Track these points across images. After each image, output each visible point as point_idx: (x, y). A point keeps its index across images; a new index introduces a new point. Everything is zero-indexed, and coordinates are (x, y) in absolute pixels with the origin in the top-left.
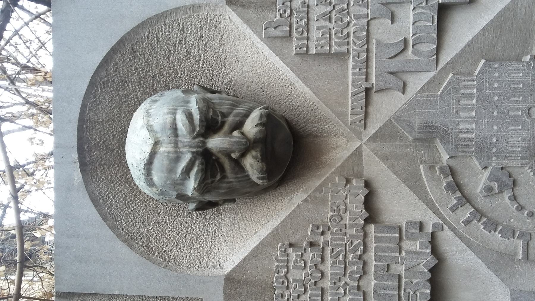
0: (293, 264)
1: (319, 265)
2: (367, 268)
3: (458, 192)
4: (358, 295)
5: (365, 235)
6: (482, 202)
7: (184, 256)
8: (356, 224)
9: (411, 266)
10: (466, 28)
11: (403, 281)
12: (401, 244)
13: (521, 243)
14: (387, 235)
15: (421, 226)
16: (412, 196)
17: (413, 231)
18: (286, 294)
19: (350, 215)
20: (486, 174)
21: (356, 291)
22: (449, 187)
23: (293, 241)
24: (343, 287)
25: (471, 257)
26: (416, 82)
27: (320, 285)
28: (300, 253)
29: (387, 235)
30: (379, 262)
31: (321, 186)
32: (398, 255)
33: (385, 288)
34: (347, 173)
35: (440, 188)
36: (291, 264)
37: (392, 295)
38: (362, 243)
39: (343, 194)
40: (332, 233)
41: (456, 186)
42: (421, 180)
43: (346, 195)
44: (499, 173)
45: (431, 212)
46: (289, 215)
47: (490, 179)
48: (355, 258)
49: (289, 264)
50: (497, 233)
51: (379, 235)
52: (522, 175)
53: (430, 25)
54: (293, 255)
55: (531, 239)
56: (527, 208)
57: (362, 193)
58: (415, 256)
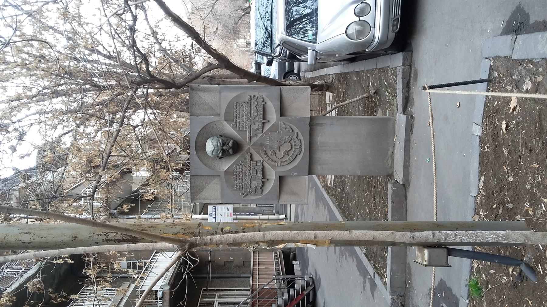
6: (271, 157)
10: (268, 127)
26: (259, 136)
53: (261, 126)
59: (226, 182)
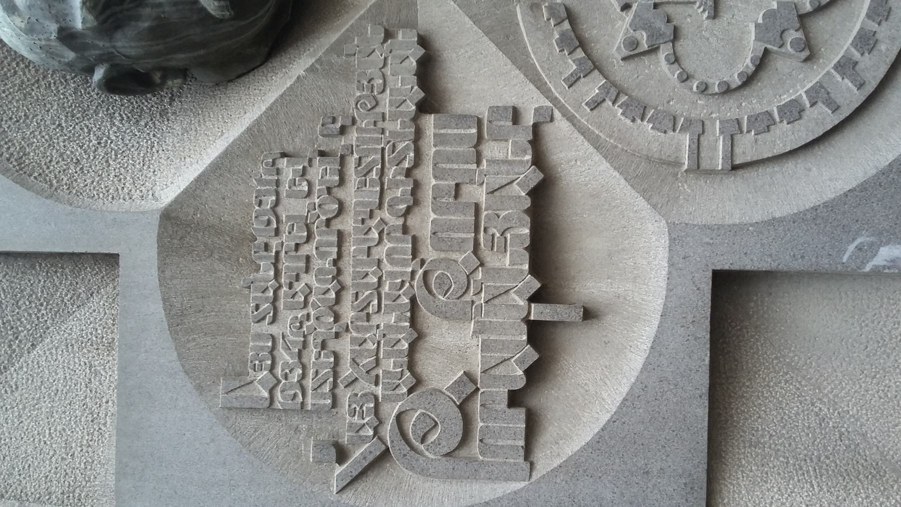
0: (287, 188)
1: (335, 190)
2: (420, 195)
3: (579, 50)
4: (403, 241)
5: (418, 134)
6: (623, 72)
7: (89, 181)
8: (401, 112)
9: (497, 186)
11: (484, 214)
12: (480, 148)
13: (686, 140)
14: (455, 131)
15: (516, 115)
16: (500, 60)
17: (502, 123)
18: (274, 243)
19: (391, 95)
20: (629, 17)
21: (399, 234)
22: (563, 41)
23: (289, 149)
24: (376, 227)
25: (602, 168)
27: (337, 225)
28: (301, 167)
29: (455, 131)
30: (442, 179)
31: (339, 42)
32: (474, 166)
33: (452, 228)
34: (387, 20)
35: (549, 45)
36: (285, 188)
37: (464, 240)
38: (412, 146)
39: (378, 57)
40: (360, 130)
41: (577, 40)
42: (517, 31)
43: (385, 59)
44: (650, 14)
45: (532, 86)
46: (282, 96)
47: (634, 26)
48: (400, 174)
49: (281, 189)
50: (645, 123)
51: (442, 131)
52: (689, 20)
54: (288, 170)
55: (703, 132)
56: (696, 76)
57: (413, 54)
58: (504, 168)
59: (177, 319)
